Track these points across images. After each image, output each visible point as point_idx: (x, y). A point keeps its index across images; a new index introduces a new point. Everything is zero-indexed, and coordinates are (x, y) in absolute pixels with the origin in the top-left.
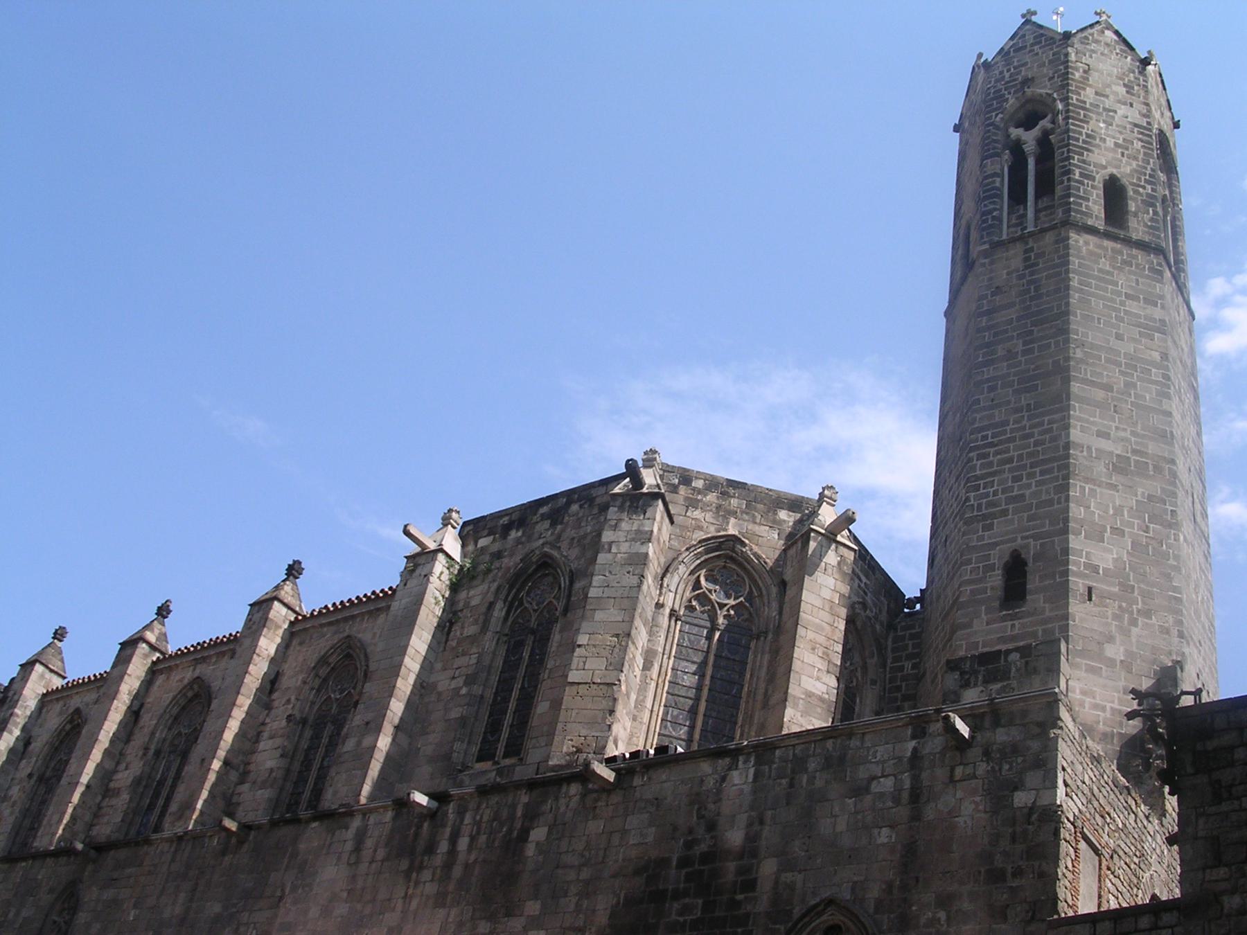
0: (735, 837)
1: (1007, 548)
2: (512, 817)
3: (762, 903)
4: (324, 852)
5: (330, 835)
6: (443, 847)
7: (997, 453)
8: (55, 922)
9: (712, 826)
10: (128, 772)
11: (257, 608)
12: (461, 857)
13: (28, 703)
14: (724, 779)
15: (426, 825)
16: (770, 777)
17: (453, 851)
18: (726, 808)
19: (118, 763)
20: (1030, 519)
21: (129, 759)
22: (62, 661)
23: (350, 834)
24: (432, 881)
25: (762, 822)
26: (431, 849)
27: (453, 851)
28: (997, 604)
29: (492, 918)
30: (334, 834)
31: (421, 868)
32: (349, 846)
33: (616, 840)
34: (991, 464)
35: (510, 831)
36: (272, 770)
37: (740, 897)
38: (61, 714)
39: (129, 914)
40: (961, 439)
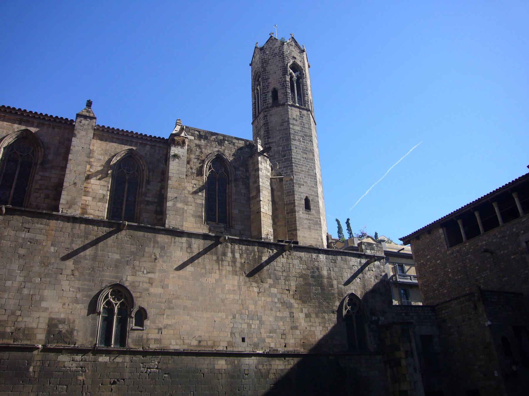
0: (325, 273)
1: (305, 195)
2: (254, 251)
3: (336, 291)
4: (173, 244)
5: (173, 239)
6: (230, 255)
7: (299, 167)
9: (318, 269)
14: (318, 256)
16: (329, 259)
18: (321, 265)
20: (310, 189)
24: (229, 265)
25: (330, 271)
26: (224, 254)
27: (234, 257)
28: (305, 209)
29: (256, 282)
30: (175, 239)
31: (222, 260)
32: (185, 245)
33: (291, 266)
34: (298, 169)
35: (254, 255)
37: (330, 289)
39: (49, 248)
40: (284, 156)
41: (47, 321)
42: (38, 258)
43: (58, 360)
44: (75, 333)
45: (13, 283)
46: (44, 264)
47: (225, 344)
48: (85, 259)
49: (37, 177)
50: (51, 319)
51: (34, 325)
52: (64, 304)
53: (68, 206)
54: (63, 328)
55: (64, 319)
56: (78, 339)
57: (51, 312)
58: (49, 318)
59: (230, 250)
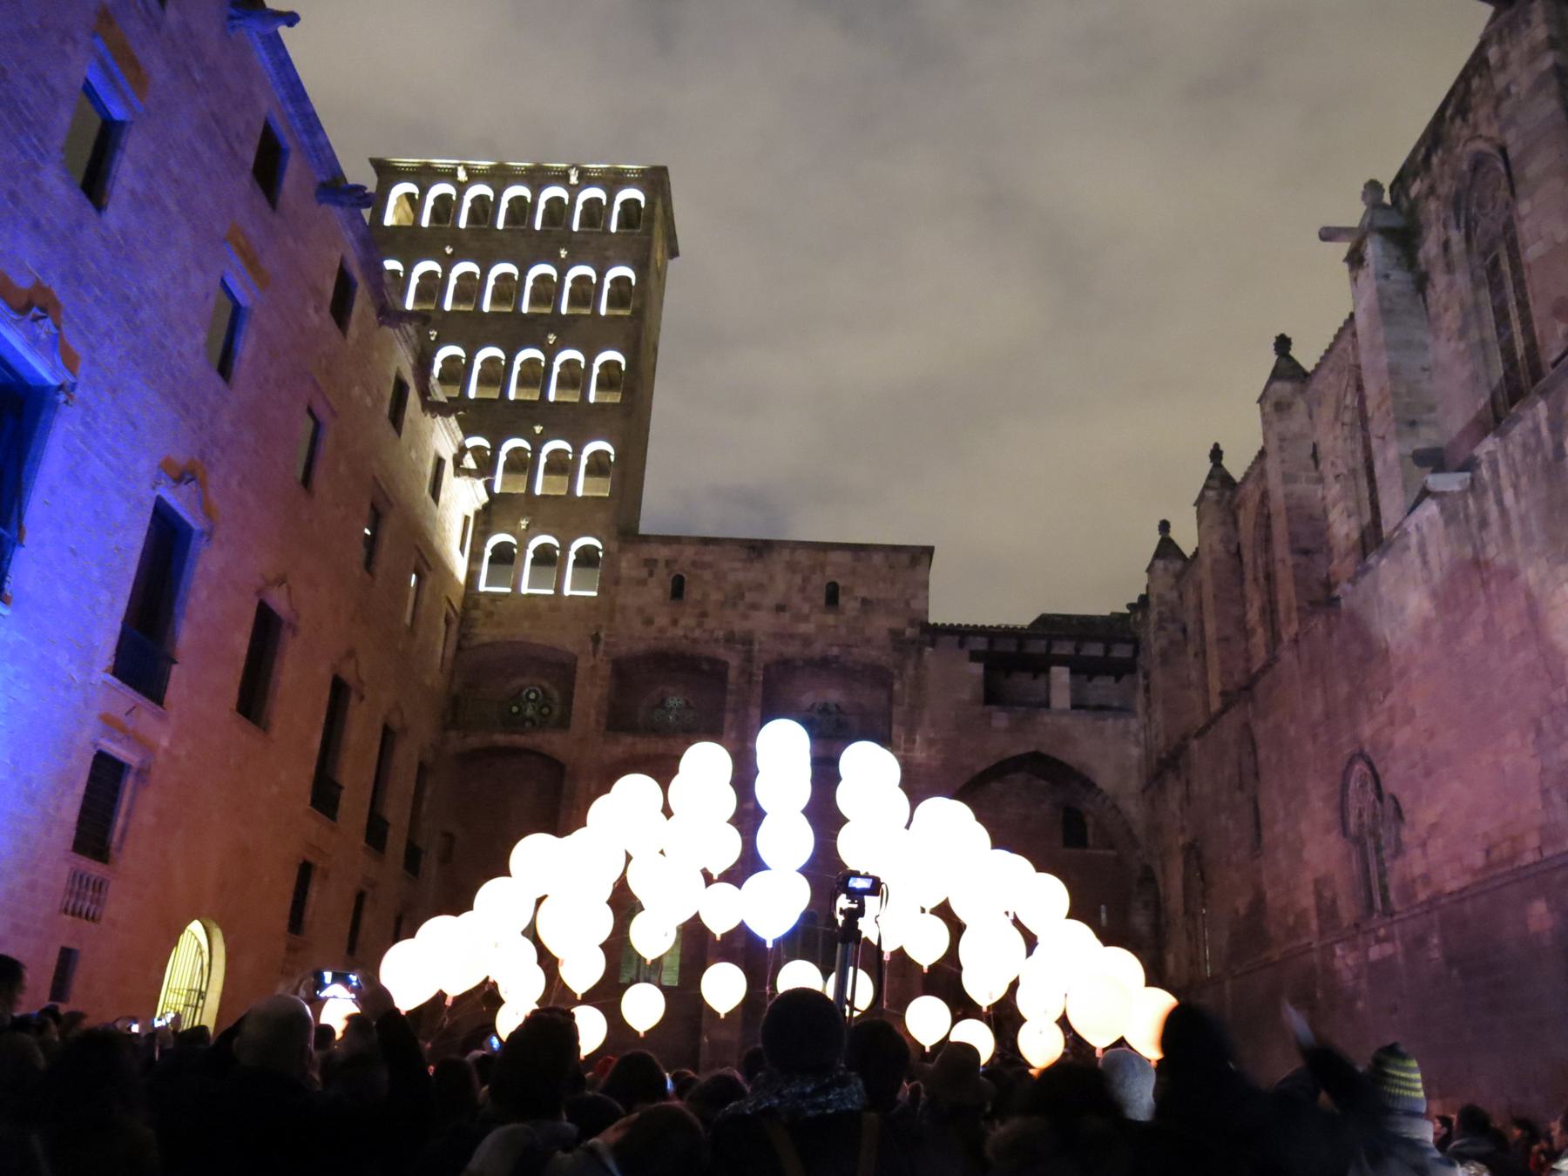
2: (1540, 442)
11: (1264, 400)
12: (1514, 515)
15: (1471, 501)
17: (1503, 512)
19: (1244, 606)
23: (1413, 553)
26: (1484, 524)
27: (1503, 512)
32: (1418, 562)
36: (1347, 536)
47: (1533, 840)
50: (1317, 882)
59: (1491, 494)
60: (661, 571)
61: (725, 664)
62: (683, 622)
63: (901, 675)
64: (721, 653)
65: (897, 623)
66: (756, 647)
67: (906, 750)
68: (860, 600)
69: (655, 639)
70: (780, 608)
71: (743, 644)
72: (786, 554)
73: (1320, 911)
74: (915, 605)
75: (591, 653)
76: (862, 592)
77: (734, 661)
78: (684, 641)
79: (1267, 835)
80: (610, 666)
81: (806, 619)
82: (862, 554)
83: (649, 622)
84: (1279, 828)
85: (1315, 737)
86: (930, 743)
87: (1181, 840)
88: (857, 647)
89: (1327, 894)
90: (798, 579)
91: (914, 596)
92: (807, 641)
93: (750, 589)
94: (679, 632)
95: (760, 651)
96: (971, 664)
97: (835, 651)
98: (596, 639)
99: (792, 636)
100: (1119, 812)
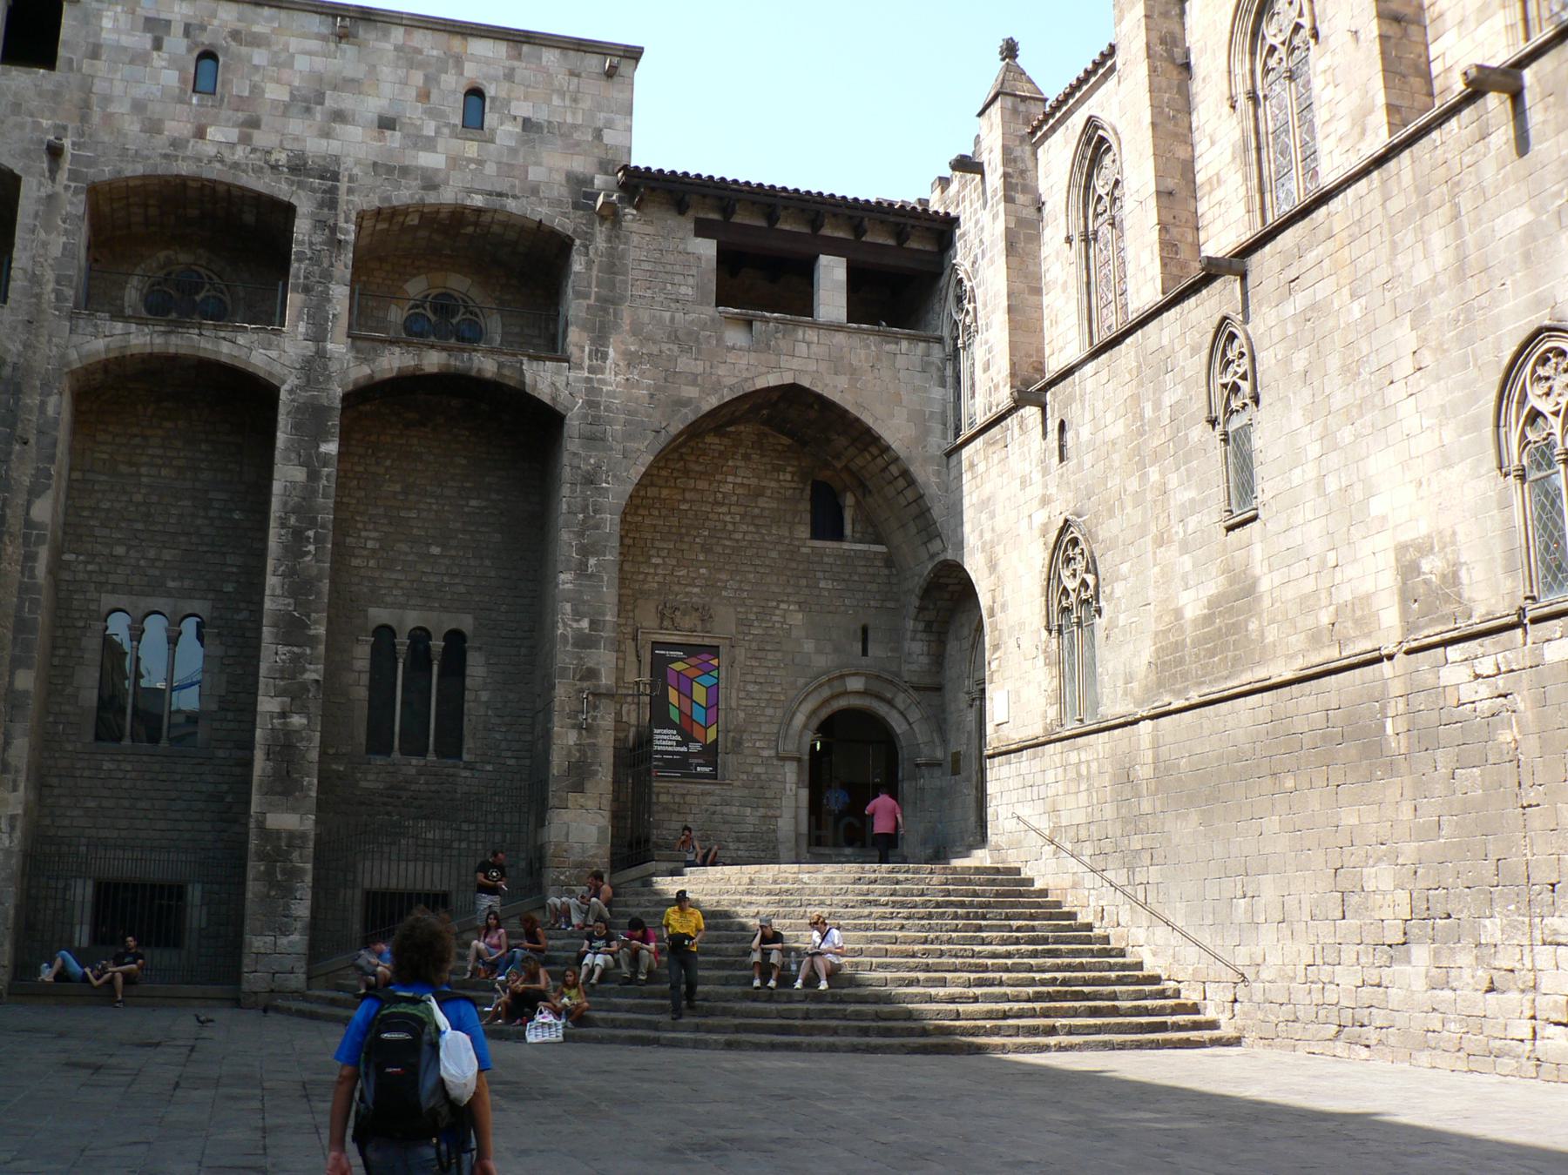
8: (1224, 386)
10: (1217, 146)
13: (1015, 154)
21: (1208, 129)
22: (1030, 81)
38: (1067, 142)
39: (1350, 311)
41: (1391, 557)
42: (1334, 362)
43: (1442, 684)
44: (1464, 575)
45: (1304, 471)
46: (1350, 372)
48: (1437, 289)
49: (1317, 83)
50: (1402, 549)
51: (1368, 586)
52: (1421, 483)
53: (1358, 129)
54: (1431, 566)
55: (1429, 536)
56: (1474, 595)
57: (1396, 526)
58: (1396, 548)
60: (176, 43)
61: (289, 210)
62: (213, 133)
63: (587, 247)
64: (281, 189)
65: (580, 165)
66: (343, 185)
67: (592, 370)
68: (520, 120)
69: (166, 156)
70: (386, 124)
71: (322, 178)
72: (398, 34)
73: (1406, 596)
74: (609, 137)
75: (47, 174)
76: (523, 109)
77: (305, 206)
78: (218, 165)
79: (1266, 487)
80: (83, 197)
81: (429, 144)
82: (525, 48)
83: (153, 128)
84: (1304, 475)
85: (1419, 316)
86: (632, 360)
87: (1040, 517)
88: (515, 197)
89: (1431, 566)
90: (418, 78)
91: (609, 125)
92: (430, 184)
93: (335, 88)
94: (211, 150)
95: (350, 191)
96: (699, 240)
97: (478, 201)
98: (55, 152)
99: (405, 171)
100: (911, 482)
